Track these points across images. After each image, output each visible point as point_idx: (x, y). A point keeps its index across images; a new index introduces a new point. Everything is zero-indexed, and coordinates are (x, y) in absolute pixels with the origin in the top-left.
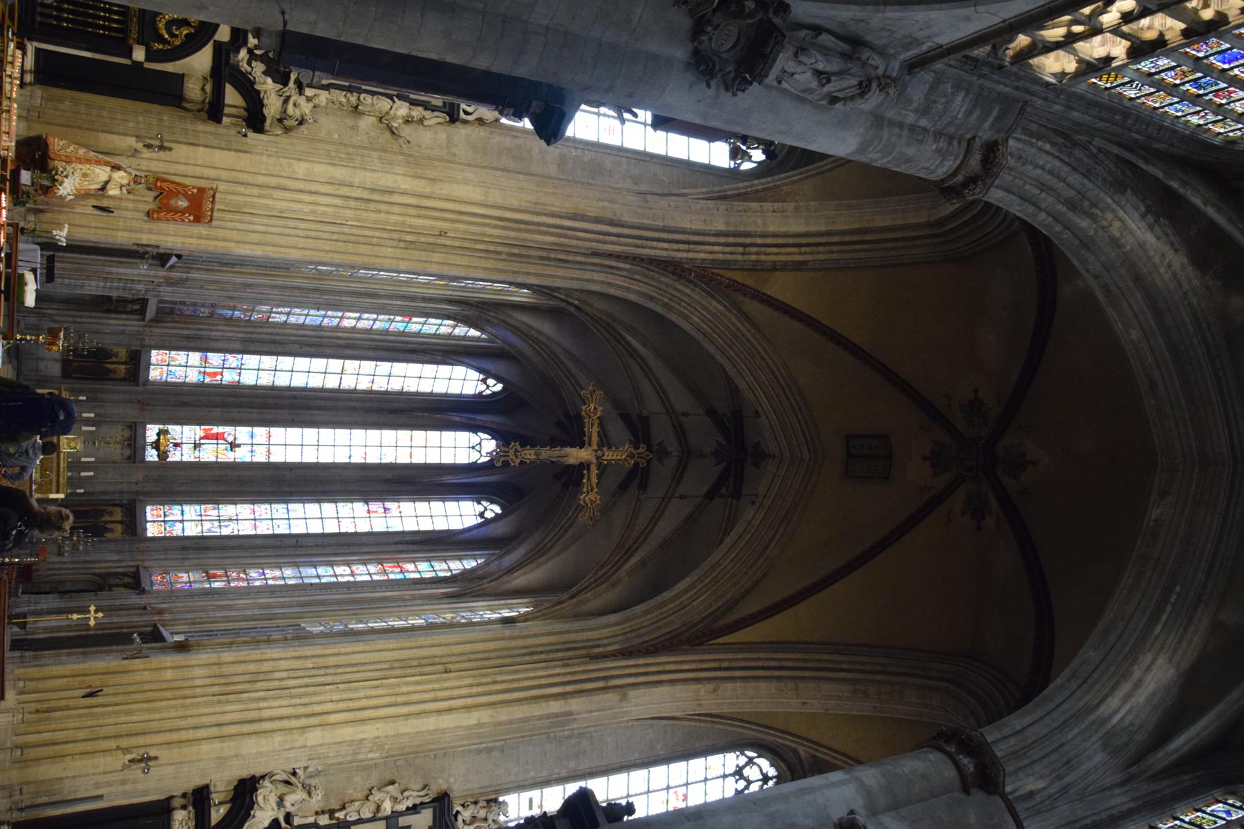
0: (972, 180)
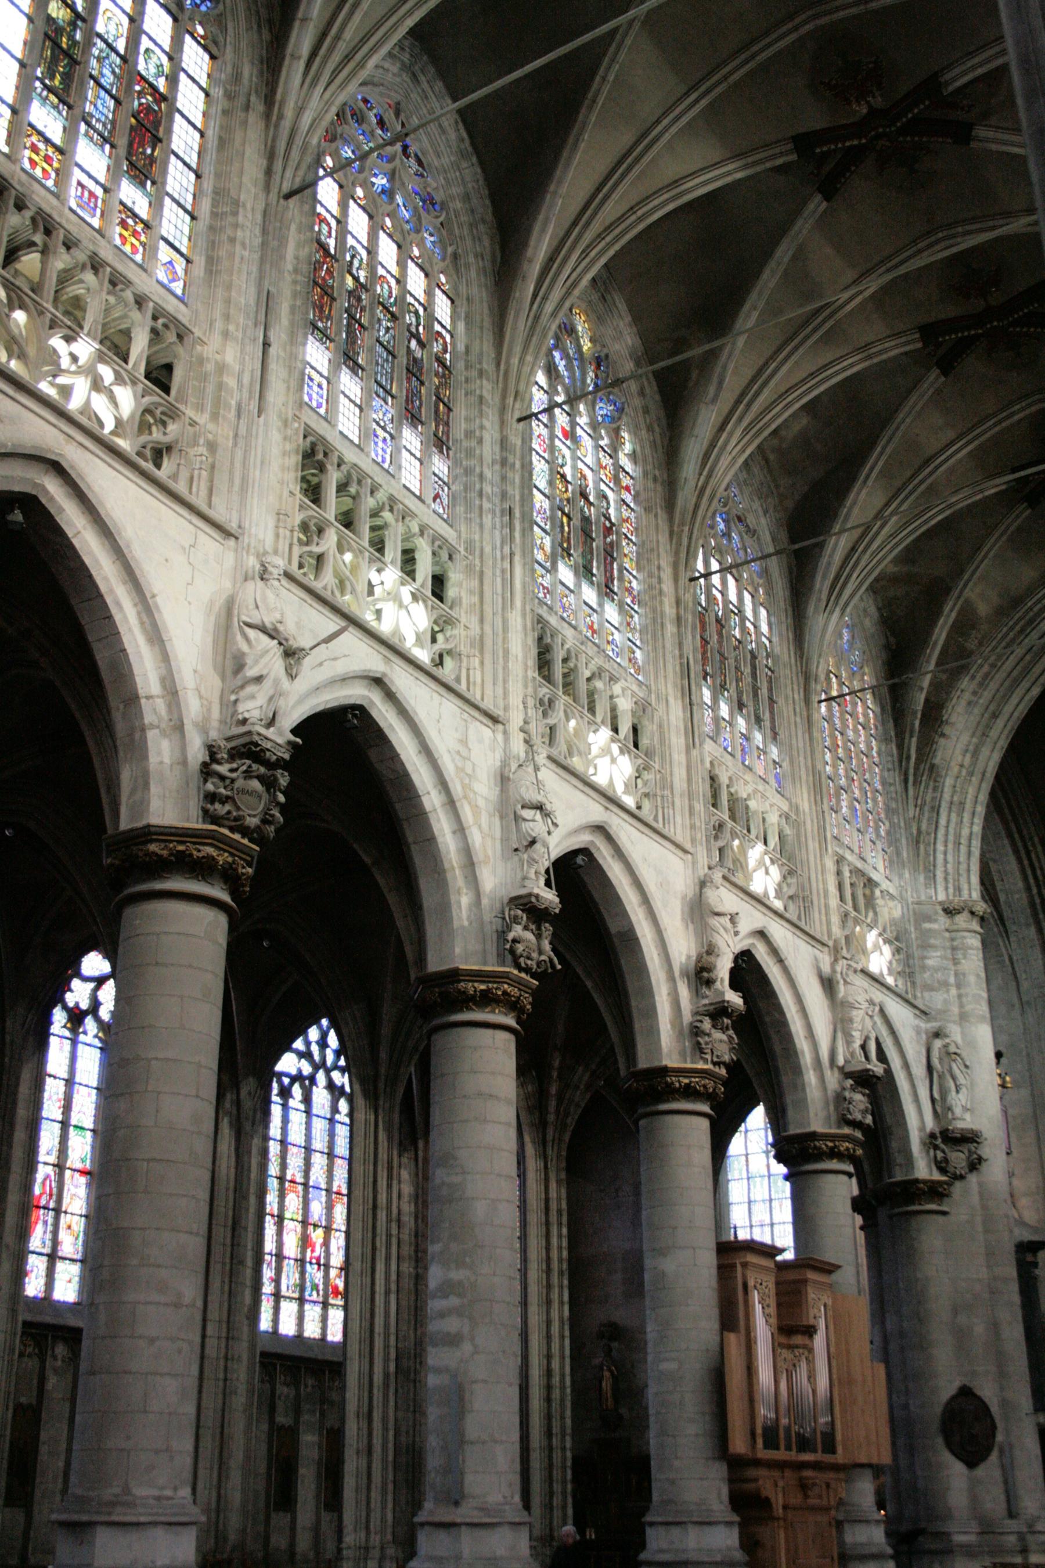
0: (972, 913)
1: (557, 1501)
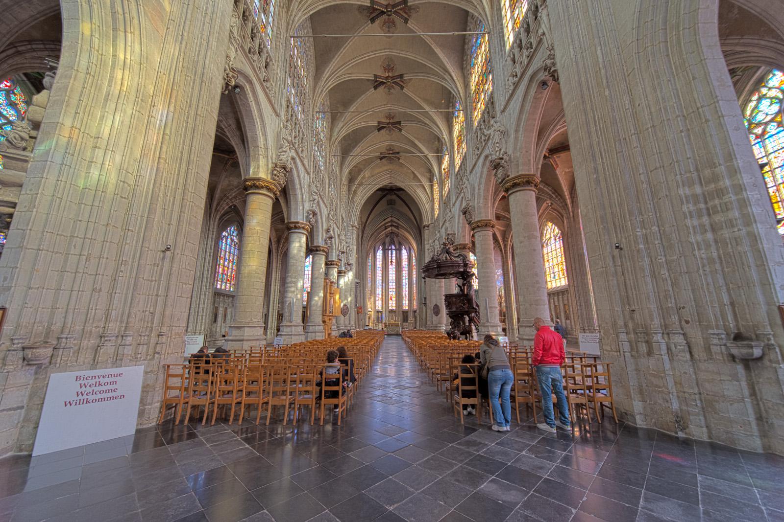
1: (274, 321)
